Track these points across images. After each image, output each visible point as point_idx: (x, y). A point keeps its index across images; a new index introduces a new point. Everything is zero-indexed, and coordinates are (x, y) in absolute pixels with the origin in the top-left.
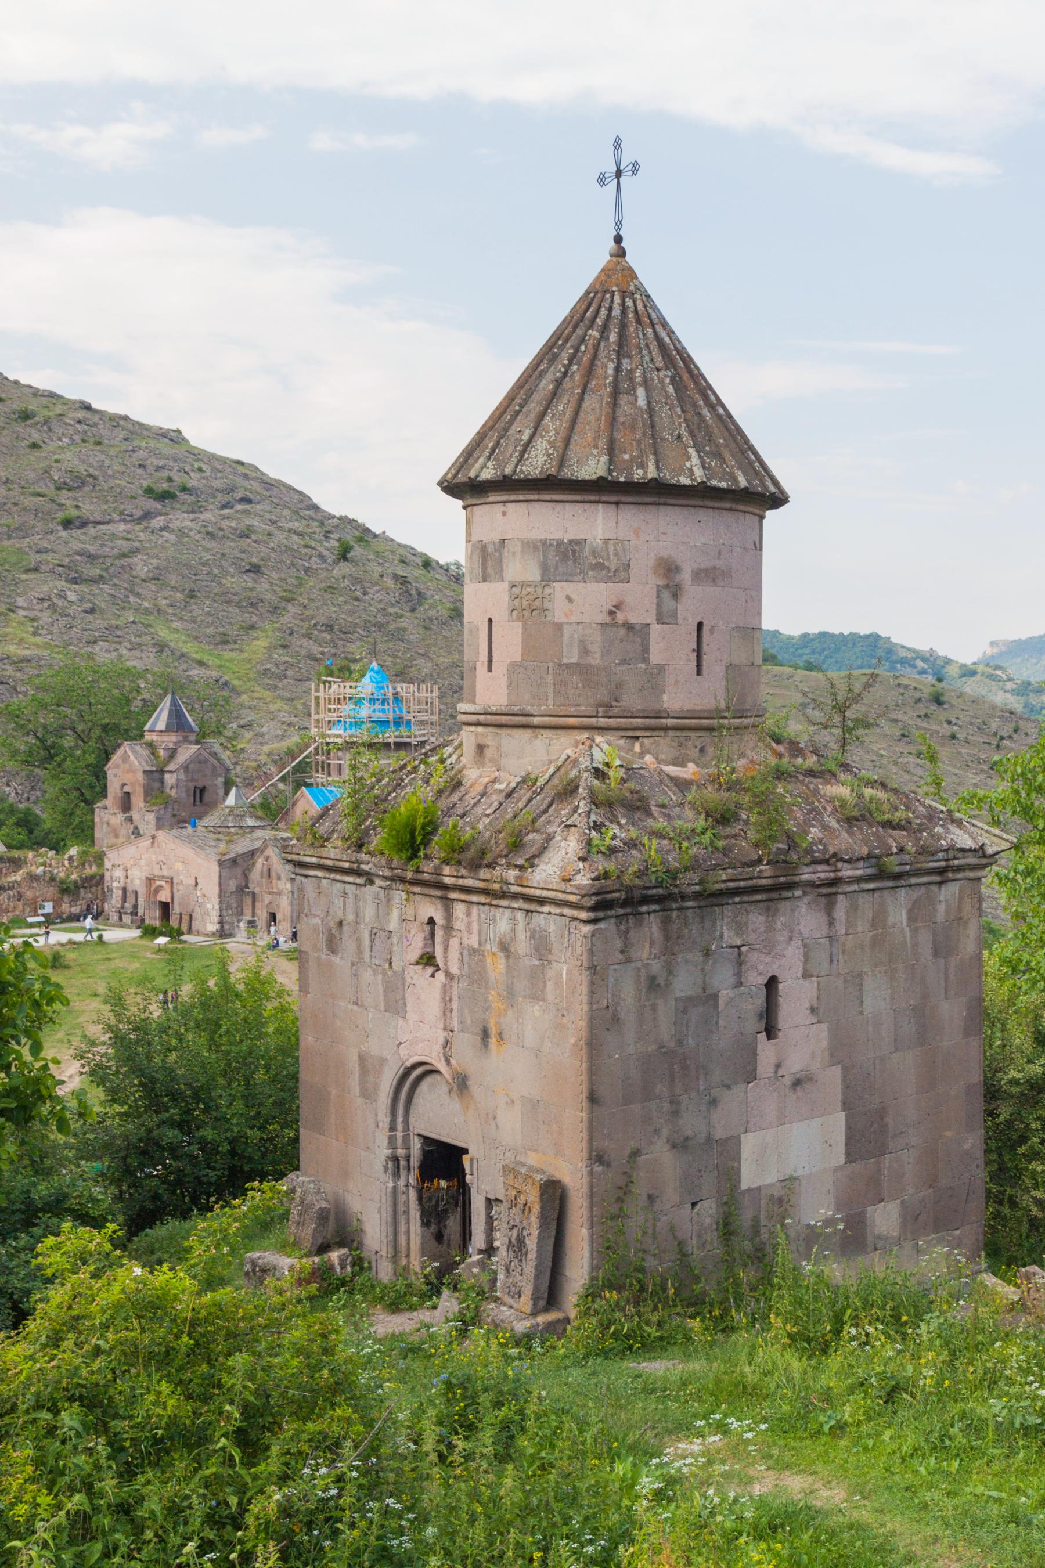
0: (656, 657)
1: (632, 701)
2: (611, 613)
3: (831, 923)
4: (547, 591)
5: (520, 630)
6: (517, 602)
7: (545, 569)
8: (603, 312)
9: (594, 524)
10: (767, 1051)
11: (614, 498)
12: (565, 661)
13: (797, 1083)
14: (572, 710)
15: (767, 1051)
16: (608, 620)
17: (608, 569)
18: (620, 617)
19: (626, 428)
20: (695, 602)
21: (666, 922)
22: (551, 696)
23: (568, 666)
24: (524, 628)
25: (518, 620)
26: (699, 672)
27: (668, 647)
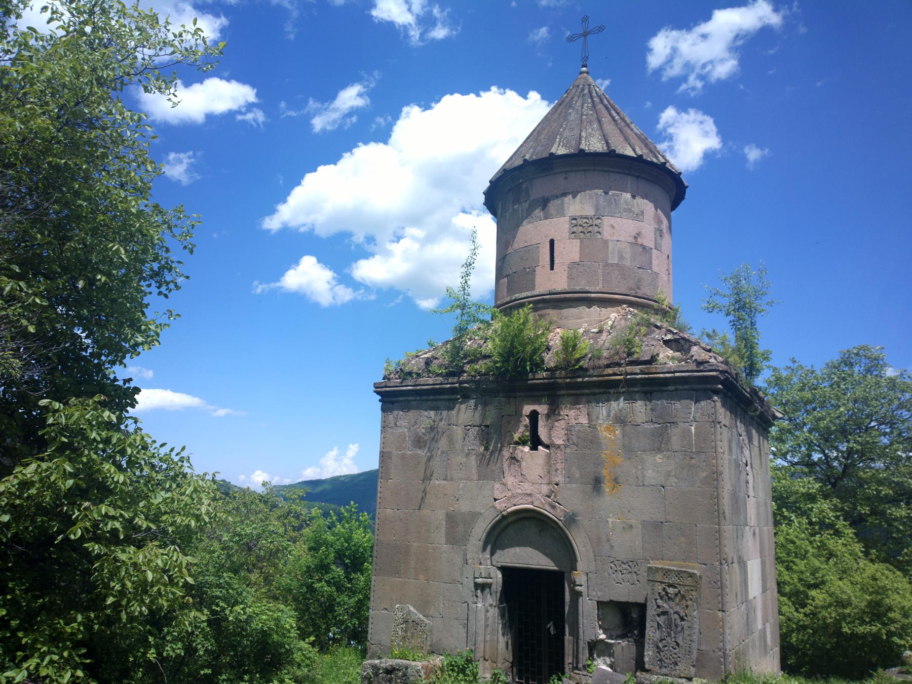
0: (655, 269)
1: (646, 291)
2: (635, 238)
4: (600, 221)
5: (578, 244)
6: (575, 229)
7: (597, 208)
12: (610, 262)
14: (617, 290)
16: (633, 241)
17: (633, 212)
18: (640, 241)
22: (601, 282)
23: (612, 265)
24: (582, 243)
25: (575, 238)
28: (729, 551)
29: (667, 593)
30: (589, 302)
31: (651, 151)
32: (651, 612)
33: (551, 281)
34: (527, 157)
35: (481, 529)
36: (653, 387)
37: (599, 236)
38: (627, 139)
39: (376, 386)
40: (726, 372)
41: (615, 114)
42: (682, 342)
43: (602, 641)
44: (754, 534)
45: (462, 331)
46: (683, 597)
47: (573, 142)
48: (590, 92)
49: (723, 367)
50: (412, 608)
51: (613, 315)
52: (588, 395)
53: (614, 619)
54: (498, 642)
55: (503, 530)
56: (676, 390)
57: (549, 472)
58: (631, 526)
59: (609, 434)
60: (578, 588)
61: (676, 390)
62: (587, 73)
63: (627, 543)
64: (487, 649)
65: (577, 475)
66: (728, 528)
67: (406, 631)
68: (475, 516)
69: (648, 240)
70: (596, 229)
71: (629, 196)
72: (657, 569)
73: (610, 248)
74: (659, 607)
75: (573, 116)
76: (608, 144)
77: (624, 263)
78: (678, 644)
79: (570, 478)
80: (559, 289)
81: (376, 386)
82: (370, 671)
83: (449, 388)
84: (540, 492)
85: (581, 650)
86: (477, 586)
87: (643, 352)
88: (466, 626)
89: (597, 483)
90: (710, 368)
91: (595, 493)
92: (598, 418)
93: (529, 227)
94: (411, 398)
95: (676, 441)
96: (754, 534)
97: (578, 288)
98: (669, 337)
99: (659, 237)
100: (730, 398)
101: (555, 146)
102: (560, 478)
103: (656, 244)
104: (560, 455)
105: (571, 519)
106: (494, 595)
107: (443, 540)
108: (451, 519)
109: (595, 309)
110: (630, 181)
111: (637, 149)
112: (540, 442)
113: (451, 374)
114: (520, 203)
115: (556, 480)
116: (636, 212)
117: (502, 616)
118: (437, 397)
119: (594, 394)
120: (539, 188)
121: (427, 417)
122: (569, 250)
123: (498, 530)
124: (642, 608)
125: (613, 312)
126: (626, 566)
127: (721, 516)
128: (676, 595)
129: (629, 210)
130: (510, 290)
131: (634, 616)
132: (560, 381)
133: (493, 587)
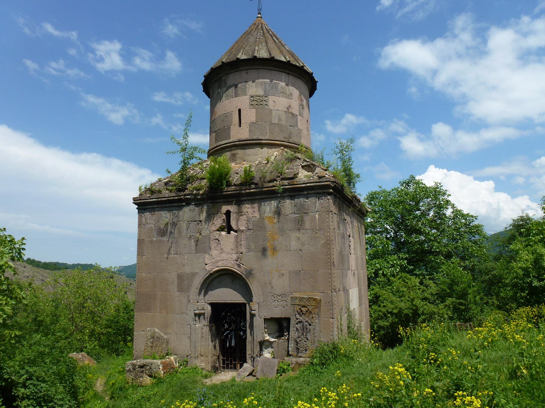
1: (294, 139)
6: (253, 103)
7: (265, 91)
11: (288, 72)
12: (273, 122)
14: (277, 139)
18: (290, 110)
23: (274, 124)
25: (253, 108)
28: (337, 284)
29: (302, 311)
30: (261, 145)
31: (296, 60)
32: (293, 322)
34: (224, 61)
35: (198, 282)
36: (296, 192)
37: (267, 107)
38: (281, 52)
39: (135, 199)
40: (335, 182)
41: (275, 39)
42: (312, 166)
43: (267, 340)
44: (354, 274)
45: (185, 163)
46: (310, 312)
47: (251, 53)
48: (262, 27)
49: (333, 179)
50: (156, 330)
51: (276, 153)
52: (259, 199)
53: (274, 327)
54: (209, 345)
55: (210, 282)
56: (308, 194)
57: (237, 247)
58: (283, 274)
60: (253, 312)
61: (308, 194)
62: (261, 18)
63: (281, 284)
64: (202, 350)
65: (253, 247)
66: (336, 272)
67: (153, 343)
68: (194, 275)
69: (295, 110)
70: (265, 103)
71: (283, 84)
72: (296, 298)
73: (273, 114)
74: (297, 319)
75: (252, 40)
76: (270, 54)
77: (281, 123)
78: (307, 339)
79: (249, 249)
80: (244, 139)
81: (135, 199)
82: (131, 367)
83: (178, 199)
84: (232, 258)
85: (255, 346)
86: (196, 315)
87: (288, 172)
88: (190, 338)
89: (264, 251)
90: (326, 180)
91: (263, 257)
92: (265, 213)
93: (227, 102)
94: (155, 206)
95: (307, 224)
96: (354, 274)
97: (255, 137)
98: (305, 164)
99: (301, 109)
100: (339, 198)
101: (240, 54)
102: (243, 250)
103: (300, 113)
104: (243, 236)
105: (250, 273)
106: (206, 320)
107: (176, 289)
108: (180, 277)
109: (265, 150)
110: (284, 76)
111: (287, 57)
113: (179, 190)
114: (221, 88)
115: (241, 251)
116: (288, 94)
117: (211, 330)
118: (171, 205)
119: (262, 199)
120: (232, 78)
121: (165, 216)
122: (249, 116)
123: (208, 282)
124: (288, 320)
125: (275, 151)
126: (280, 297)
127: (332, 265)
128: (307, 311)
129: (284, 93)
130: (217, 140)
131: (285, 325)
132: (243, 192)
133: (206, 315)
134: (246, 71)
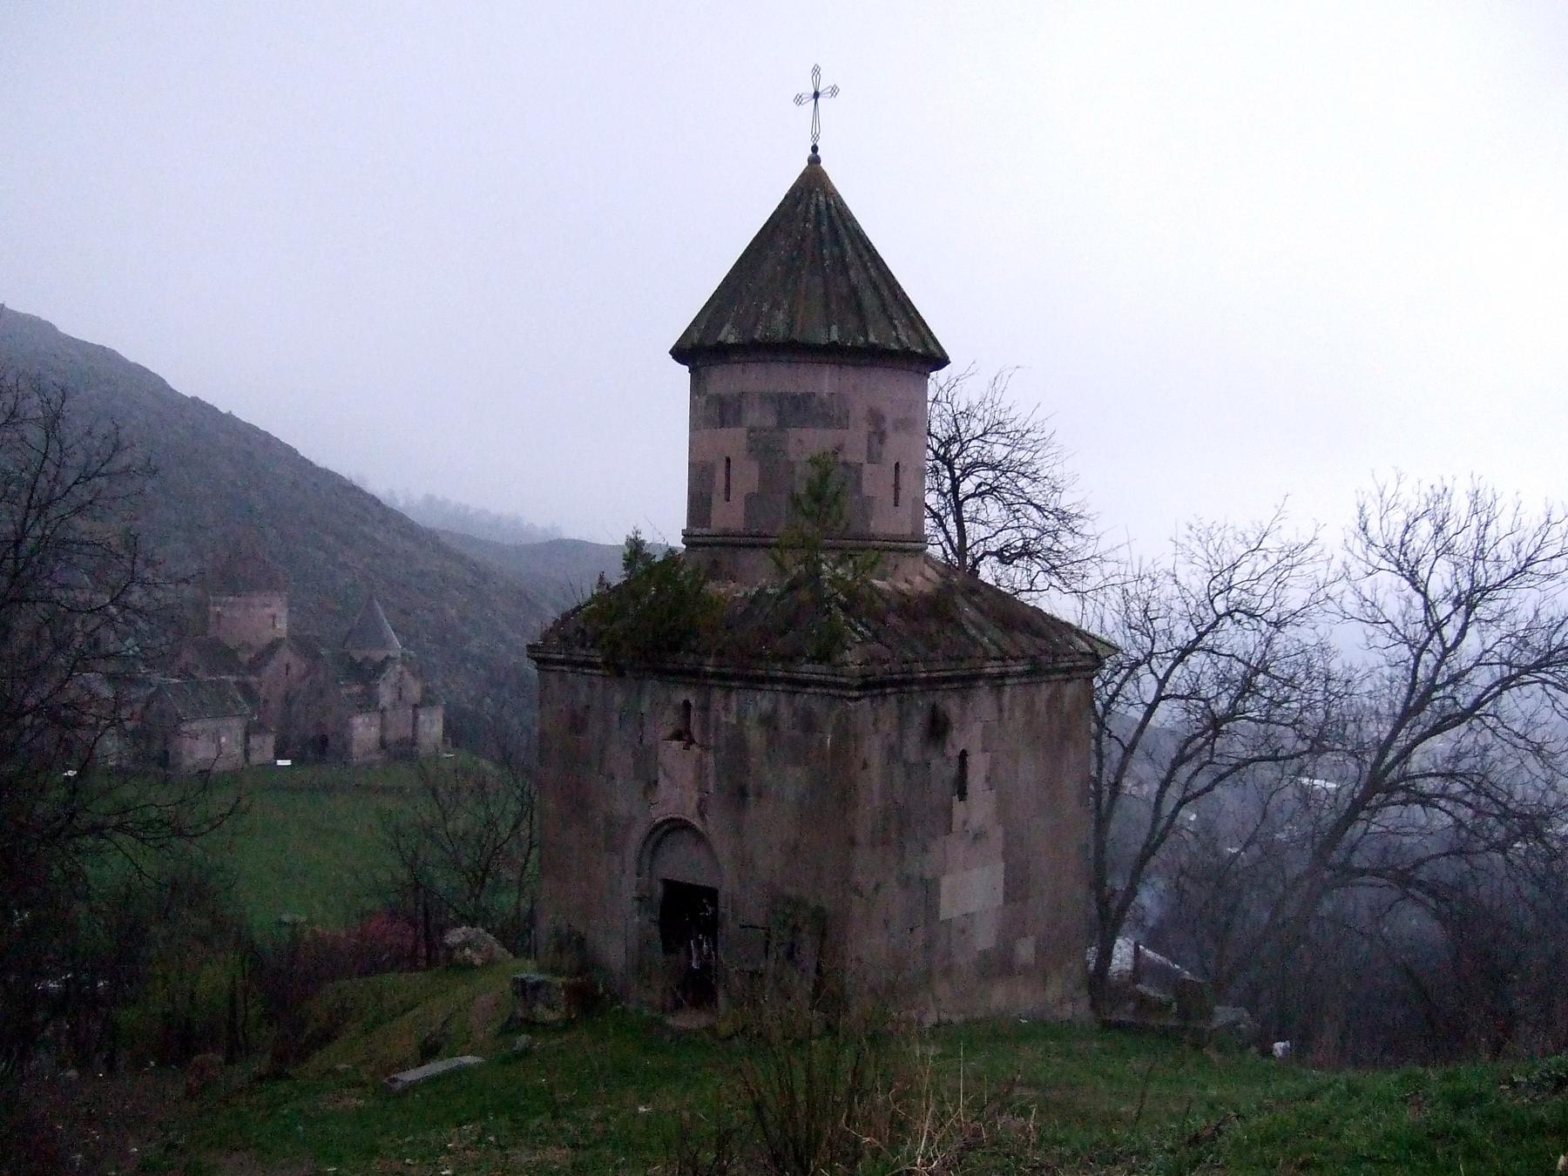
3: (1001, 710)
8: (812, 208)
9: (824, 381)
10: (958, 808)
13: (976, 837)
15: (958, 808)
18: (841, 458)
19: (809, 313)
20: (895, 444)
21: (900, 702)
24: (761, 467)
26: (896, 505)
27: (875, 483)
33: (728, 516)
59: (756, 737)
69: (856, 454)
89: (742, 792)
101: (727, 327)
112: (692, 742)
134: (740, 366)
